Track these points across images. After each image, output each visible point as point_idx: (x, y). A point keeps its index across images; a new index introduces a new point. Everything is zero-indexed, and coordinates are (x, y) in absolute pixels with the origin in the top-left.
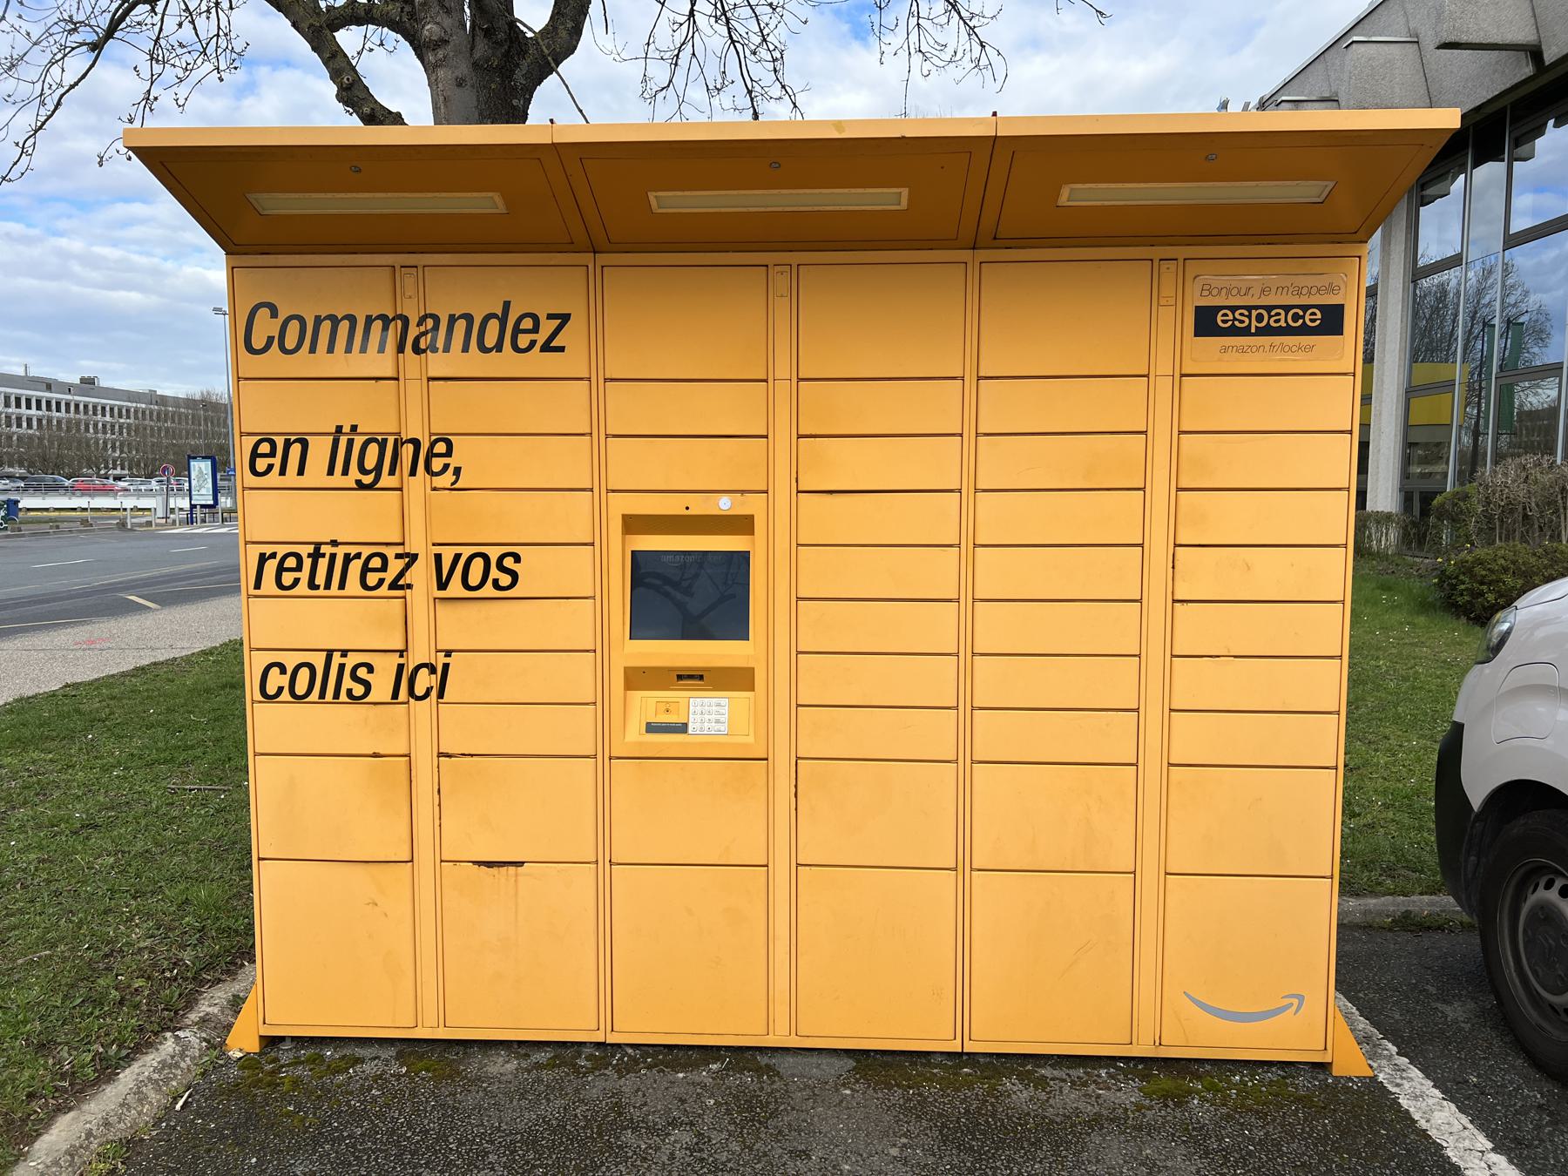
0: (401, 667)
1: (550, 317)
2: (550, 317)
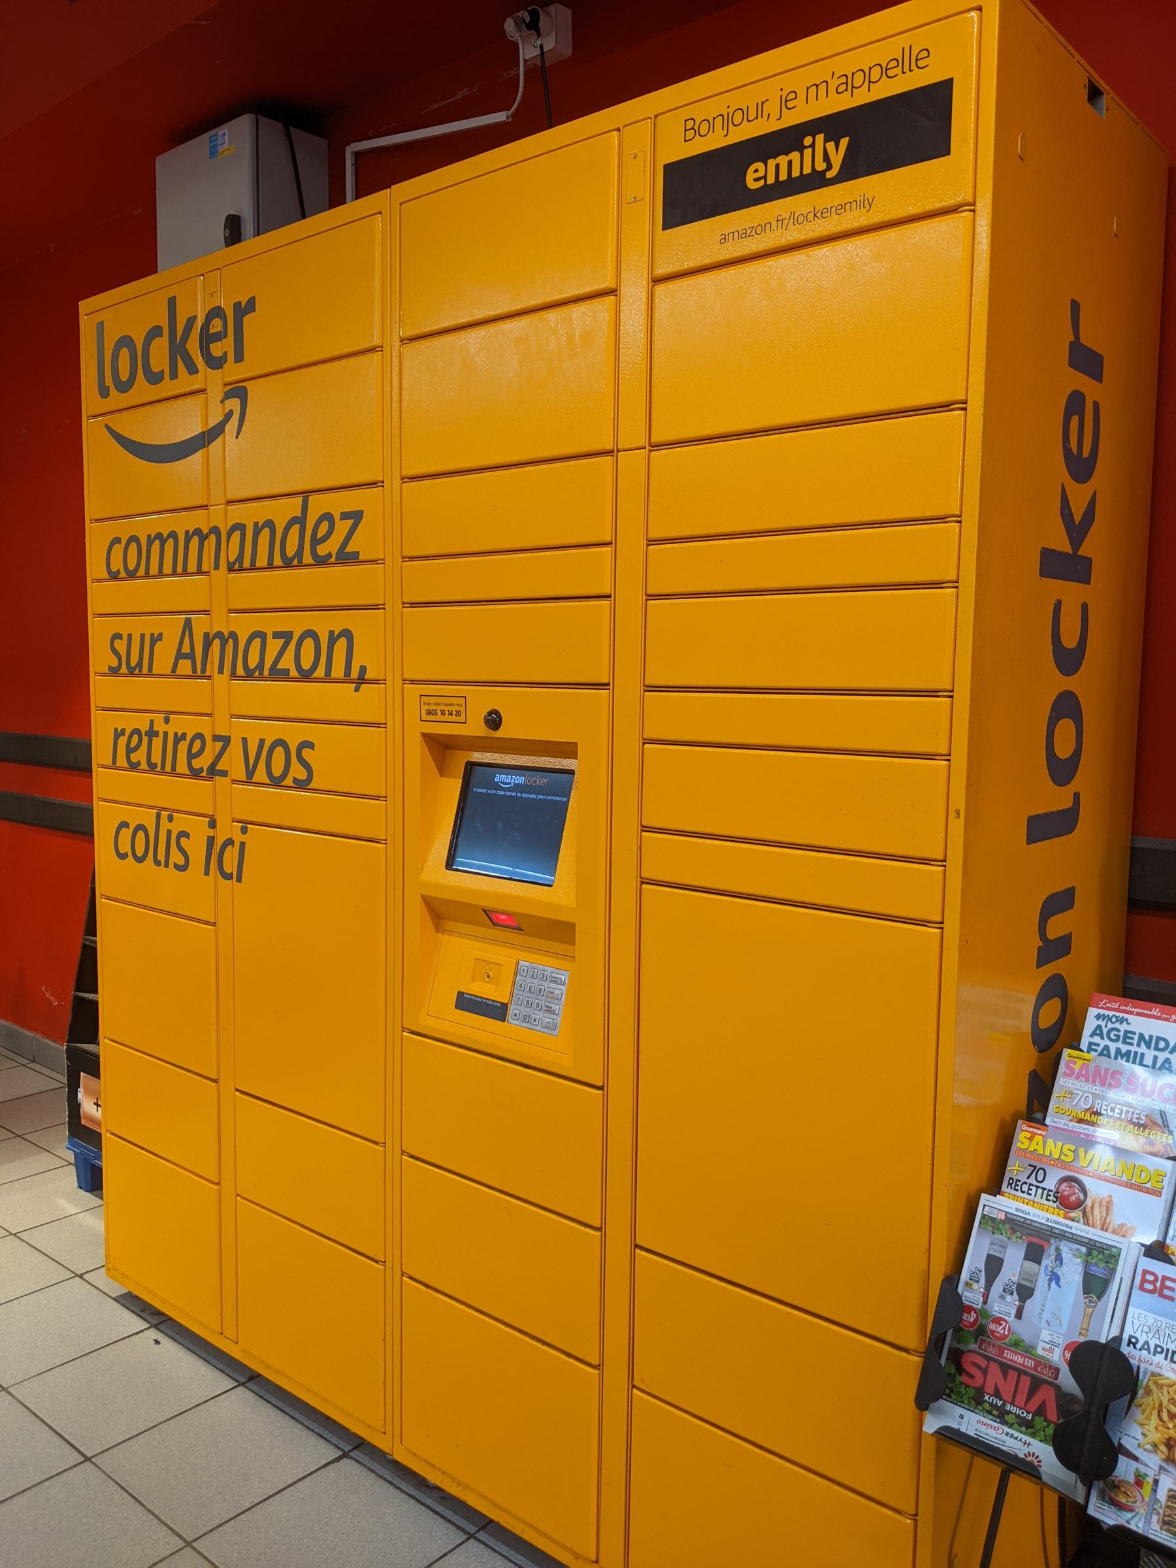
0: (211, 841)
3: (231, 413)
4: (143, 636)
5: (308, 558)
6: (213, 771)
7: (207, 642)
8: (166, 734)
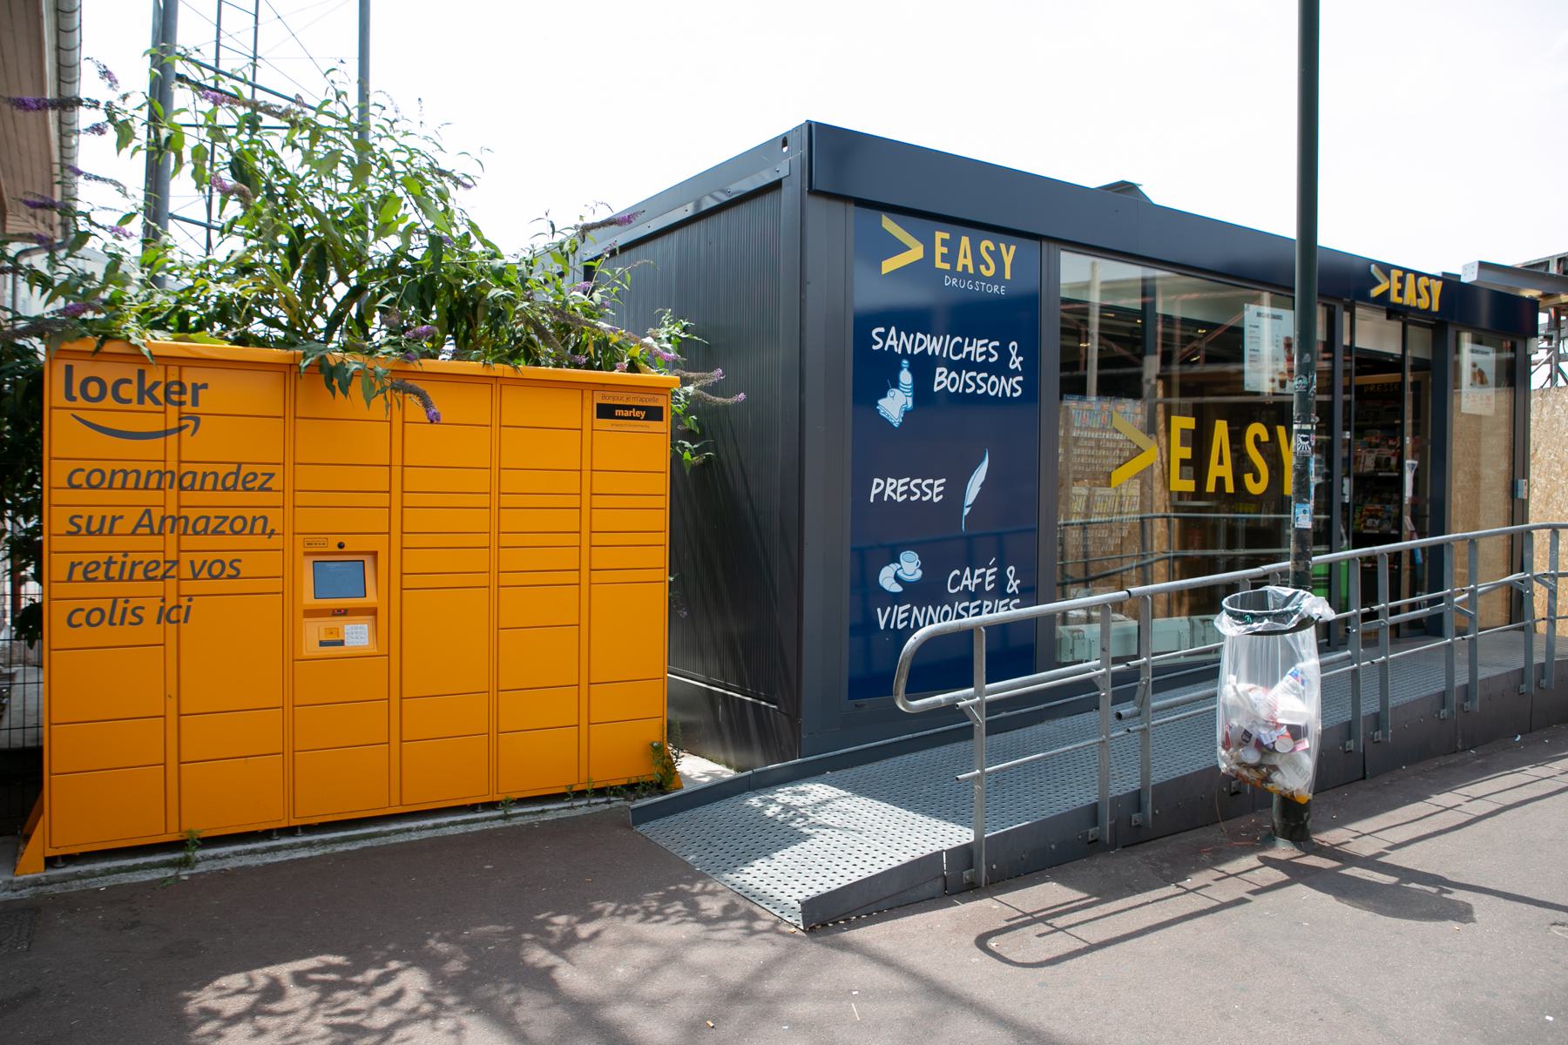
0: (162, 609)
1: (263, 474)
2: (263, 474)
3: (187, 426)
4: (104, 518)
5: (240, 486)
6: (164, 577)
7: (164, 519)
8: (124, 564)
